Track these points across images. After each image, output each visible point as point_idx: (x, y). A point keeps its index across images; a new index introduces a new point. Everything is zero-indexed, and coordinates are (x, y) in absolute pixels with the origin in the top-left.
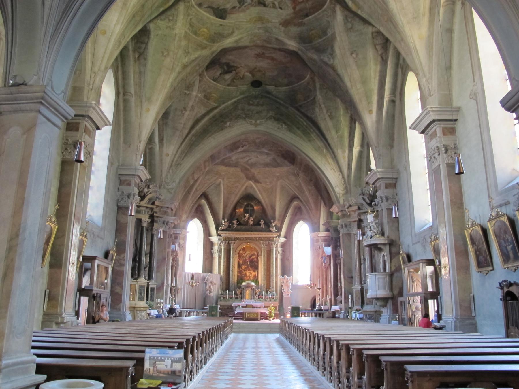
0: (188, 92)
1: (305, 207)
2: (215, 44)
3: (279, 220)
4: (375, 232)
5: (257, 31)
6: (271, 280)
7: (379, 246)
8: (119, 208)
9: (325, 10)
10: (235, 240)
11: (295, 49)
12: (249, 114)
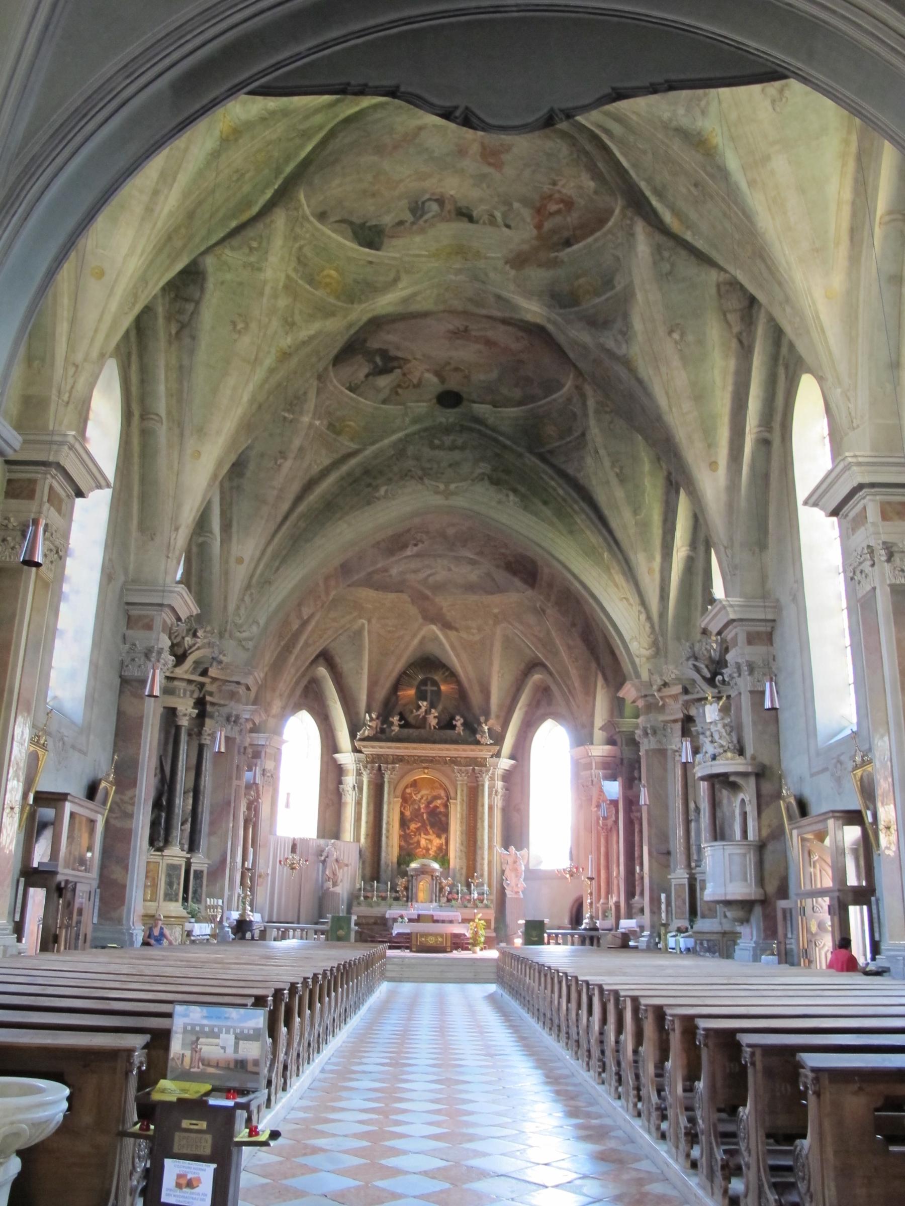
0: (291, 416)
1: (558, 685)
2: (356, 306)
3: (498, 717)
4: (722, 746)
5: (453, 277)
6: (479, 859)
7: (732, 779)
8: (125, 682)
9: (610, 231)
10: (393, 763)
11: (538, 320)
12: (431, 469)
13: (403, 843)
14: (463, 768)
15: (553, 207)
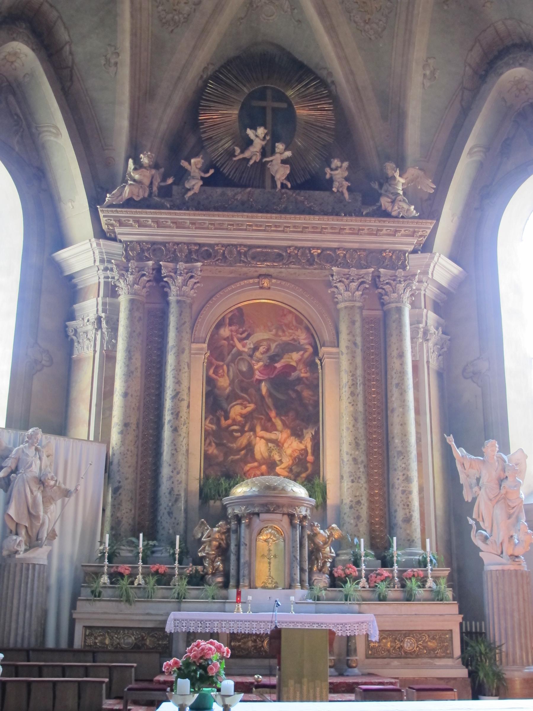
6: (397, 478)
13: (213, 450)
14: (354, 271)
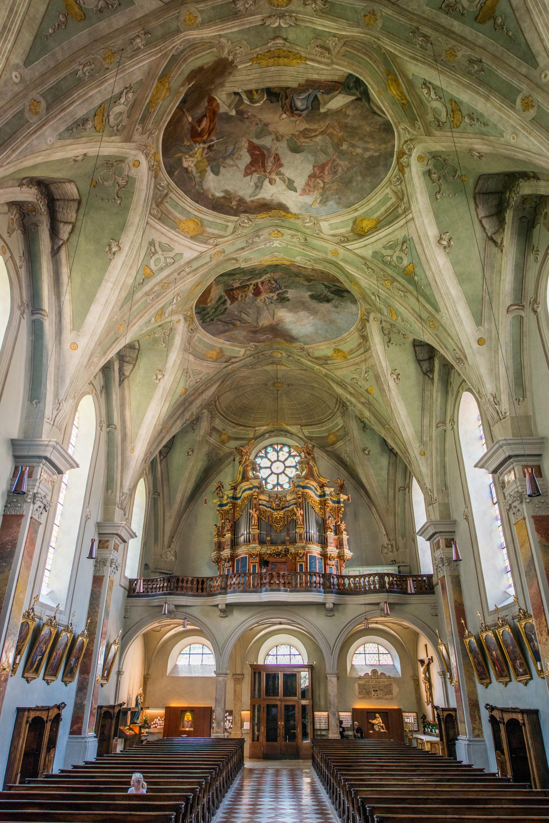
15: (205, 123)
